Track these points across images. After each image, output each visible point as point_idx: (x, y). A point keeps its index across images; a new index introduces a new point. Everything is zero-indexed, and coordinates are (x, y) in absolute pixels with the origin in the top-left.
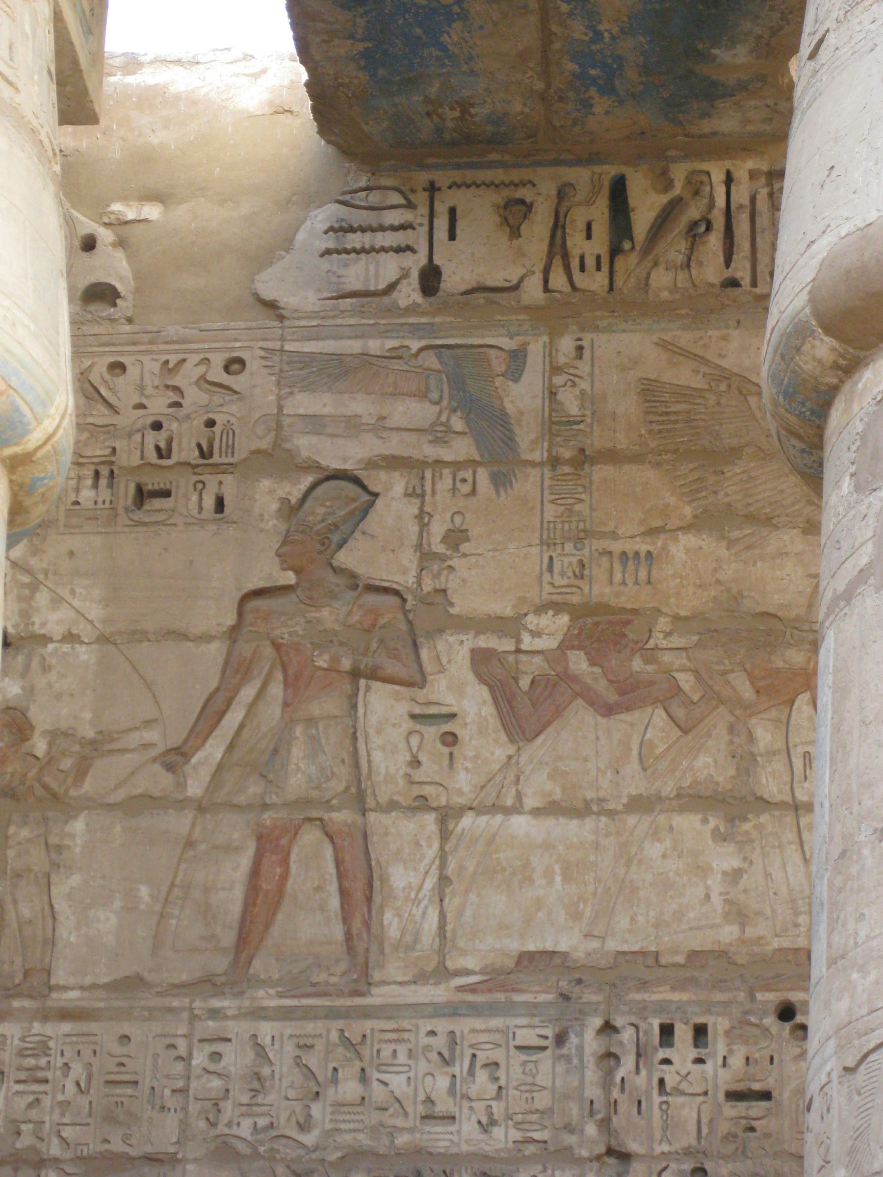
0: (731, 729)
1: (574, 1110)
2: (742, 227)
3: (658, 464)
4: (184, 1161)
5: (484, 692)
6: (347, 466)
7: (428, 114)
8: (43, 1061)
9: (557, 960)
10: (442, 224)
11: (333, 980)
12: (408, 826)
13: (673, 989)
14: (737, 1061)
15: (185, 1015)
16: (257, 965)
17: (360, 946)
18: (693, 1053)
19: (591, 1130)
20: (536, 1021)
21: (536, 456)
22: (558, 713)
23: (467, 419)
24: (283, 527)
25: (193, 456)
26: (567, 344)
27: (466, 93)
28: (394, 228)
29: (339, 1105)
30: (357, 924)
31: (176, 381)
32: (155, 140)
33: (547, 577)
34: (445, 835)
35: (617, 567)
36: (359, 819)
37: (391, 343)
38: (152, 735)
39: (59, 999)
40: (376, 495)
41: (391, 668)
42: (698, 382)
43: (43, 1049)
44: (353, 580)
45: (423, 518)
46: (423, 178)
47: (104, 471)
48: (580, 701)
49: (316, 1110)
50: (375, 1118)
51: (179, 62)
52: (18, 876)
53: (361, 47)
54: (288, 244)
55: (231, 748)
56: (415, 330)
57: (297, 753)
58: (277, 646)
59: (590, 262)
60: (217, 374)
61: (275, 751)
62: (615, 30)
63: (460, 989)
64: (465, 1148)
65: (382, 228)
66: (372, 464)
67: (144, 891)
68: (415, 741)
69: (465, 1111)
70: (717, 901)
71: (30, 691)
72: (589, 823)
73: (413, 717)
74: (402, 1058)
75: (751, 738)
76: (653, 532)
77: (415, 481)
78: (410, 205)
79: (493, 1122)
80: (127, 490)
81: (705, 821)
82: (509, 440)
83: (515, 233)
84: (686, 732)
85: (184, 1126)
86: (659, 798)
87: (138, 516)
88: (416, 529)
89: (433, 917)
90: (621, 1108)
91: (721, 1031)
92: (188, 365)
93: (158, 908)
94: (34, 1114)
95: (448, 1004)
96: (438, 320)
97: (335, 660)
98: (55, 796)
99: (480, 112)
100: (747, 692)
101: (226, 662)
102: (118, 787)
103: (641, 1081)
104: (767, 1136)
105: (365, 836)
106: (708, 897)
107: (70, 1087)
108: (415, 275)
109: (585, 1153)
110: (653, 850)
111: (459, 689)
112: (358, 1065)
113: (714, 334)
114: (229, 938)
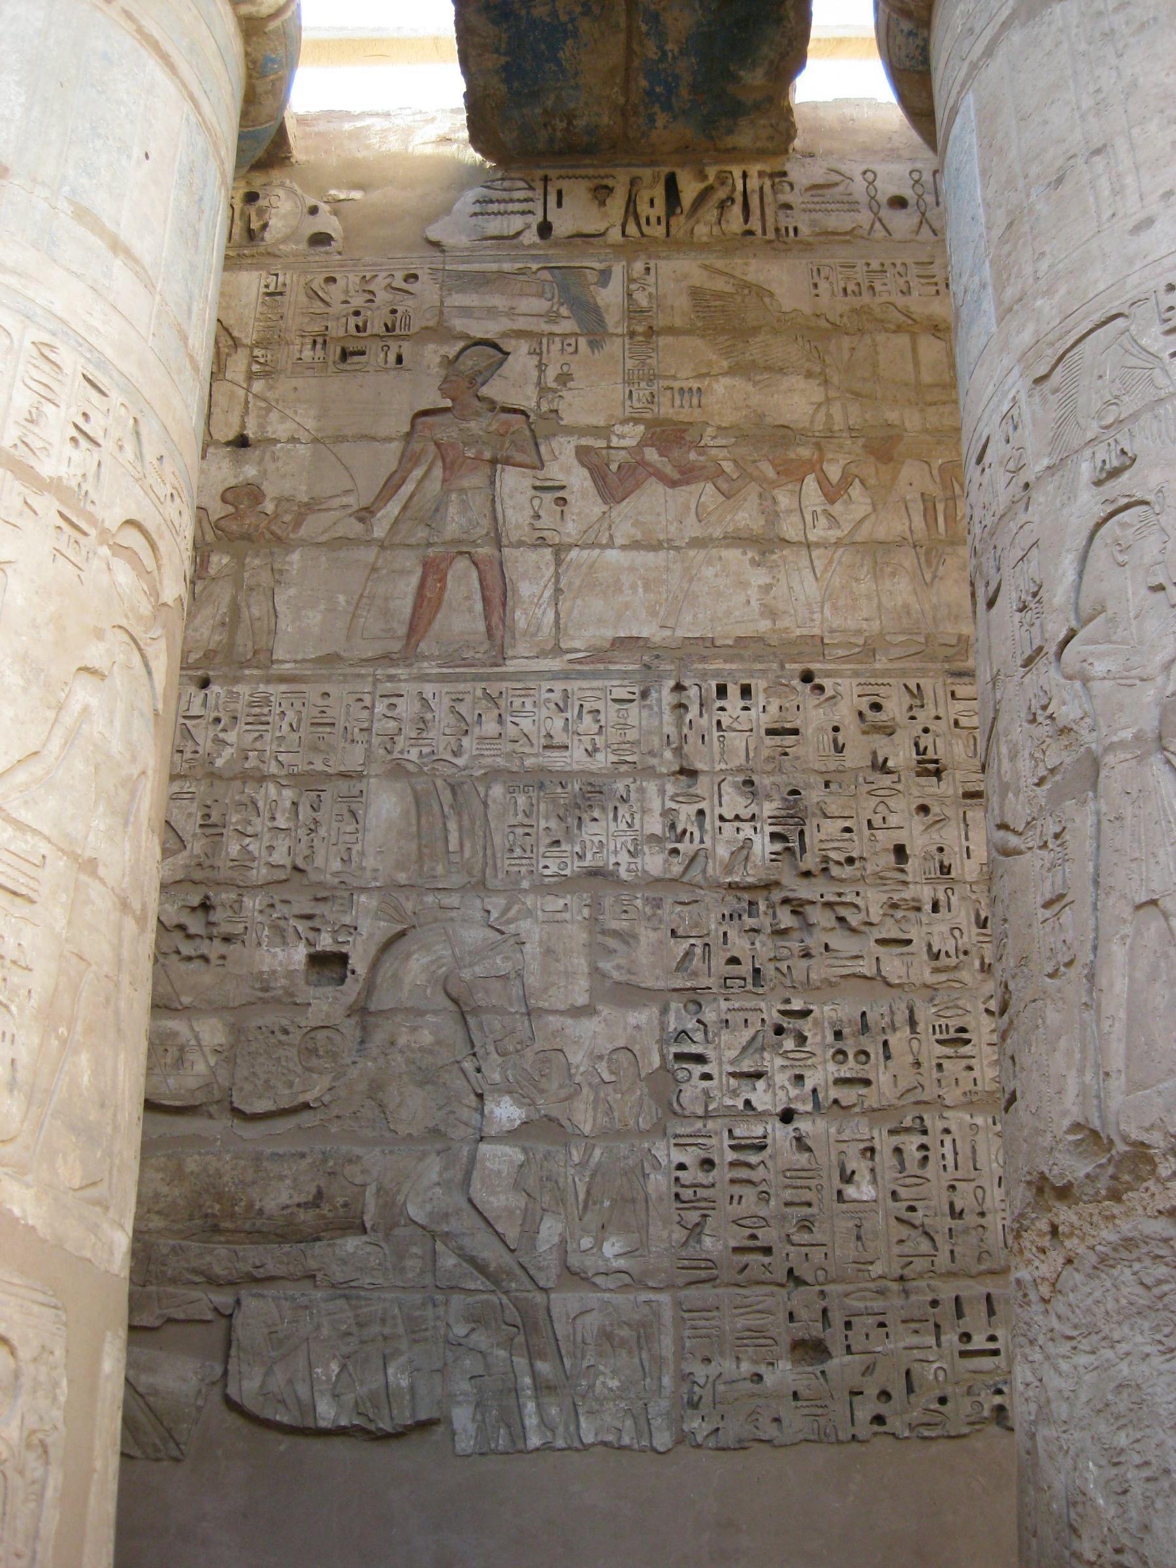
0: (760, 496)
1: (656, 742)
2: (754, 202)
3: (703, 337)
4: (368, 776)
5: (586, 472)
6: (488, 336)
7: (545, 125)
8: (266, 710)
9: (641, 643)
10: (552, 199)
11: (478, 656)
12: (532, 556)
13: (725, 661)
14: (773, 709)
15: (370, 679)
16: (423, 646)
17: (498, 634)
18: (742, 704)
19: (668, 754)
20: (626, 682)
21: (619, 331)
22: (638, 485)
23: (571, 309)
24: (443, 372)
25: (382, 331)
26: (639, 266)
27: (572, 105)
28: (519, 201)
29: (482, 739)
30: (495, 619)
31: (371, 288)
32: (359, 155)
33: (628, 403)
34: (558, 562)
35: (677, 397)
36: (496, 553)
37: (521, 265)
38: (350, 500)
39: (276, 669)
40: (508, 354)
41: (519, 457)
42: (728, 289)
43: (266, 701)
44: (492, 405)
45: (541, 367)
46: (540, 173)
47: (320, 340)
48: (653, 479)
49: (466, 742)
50: (510, 747)
51: (377, 115)
52: (251, 589)
53: (503, 60)
54: (447, 210)
55: (405, 508)
56: (535, 258)
57: (452, 510)
58: (438, 445)
59: (653, 220)
60: (399, 282)
61: (437, 510)
62: (676, 51)
63: (570, 661)
64: (575, 767)
65: (512, 201)
66: (505, 335)
67: (342, 599)
68: (536, 502)
69: (576, 743)
70: (754, 604)
71: (264, 473)
72: (662, 554)
73: (535, 488)
74: (528, 707)
75: (775, 501)
76: (700, 376)
77: (535, 345)
78: (531, 188)
79: (596, 750)
80: (335, 351)
81: (745, 553)
82: (601, 322)
83: (602, 203)
84: (728, 497)
85: (368, 753)
86: (711, 539)
87: (342, 366)
88: (535, 374)
89: (550, 616)
90: (690, 740)
91: (761, 689)
92: (379, 279)
93: (351, 609)
94: (258, 745)
95: (562, 671)
96: (550, 252)
97: (480, 452)
98: (279, 539)
99: (580, 123)
100: (771, 473)
101: (403, 455)
102: (323, 533)
103: (704, 721)
104: (798, 758)
105: (501, 564)
106: (748, 602)
107: (286, 727)
108: (534, 227)
109: (664, 770)
110: (709, 572)
111: (568, 470)
112: (496, 712)
113: (739, 261)
114: (402, 630)
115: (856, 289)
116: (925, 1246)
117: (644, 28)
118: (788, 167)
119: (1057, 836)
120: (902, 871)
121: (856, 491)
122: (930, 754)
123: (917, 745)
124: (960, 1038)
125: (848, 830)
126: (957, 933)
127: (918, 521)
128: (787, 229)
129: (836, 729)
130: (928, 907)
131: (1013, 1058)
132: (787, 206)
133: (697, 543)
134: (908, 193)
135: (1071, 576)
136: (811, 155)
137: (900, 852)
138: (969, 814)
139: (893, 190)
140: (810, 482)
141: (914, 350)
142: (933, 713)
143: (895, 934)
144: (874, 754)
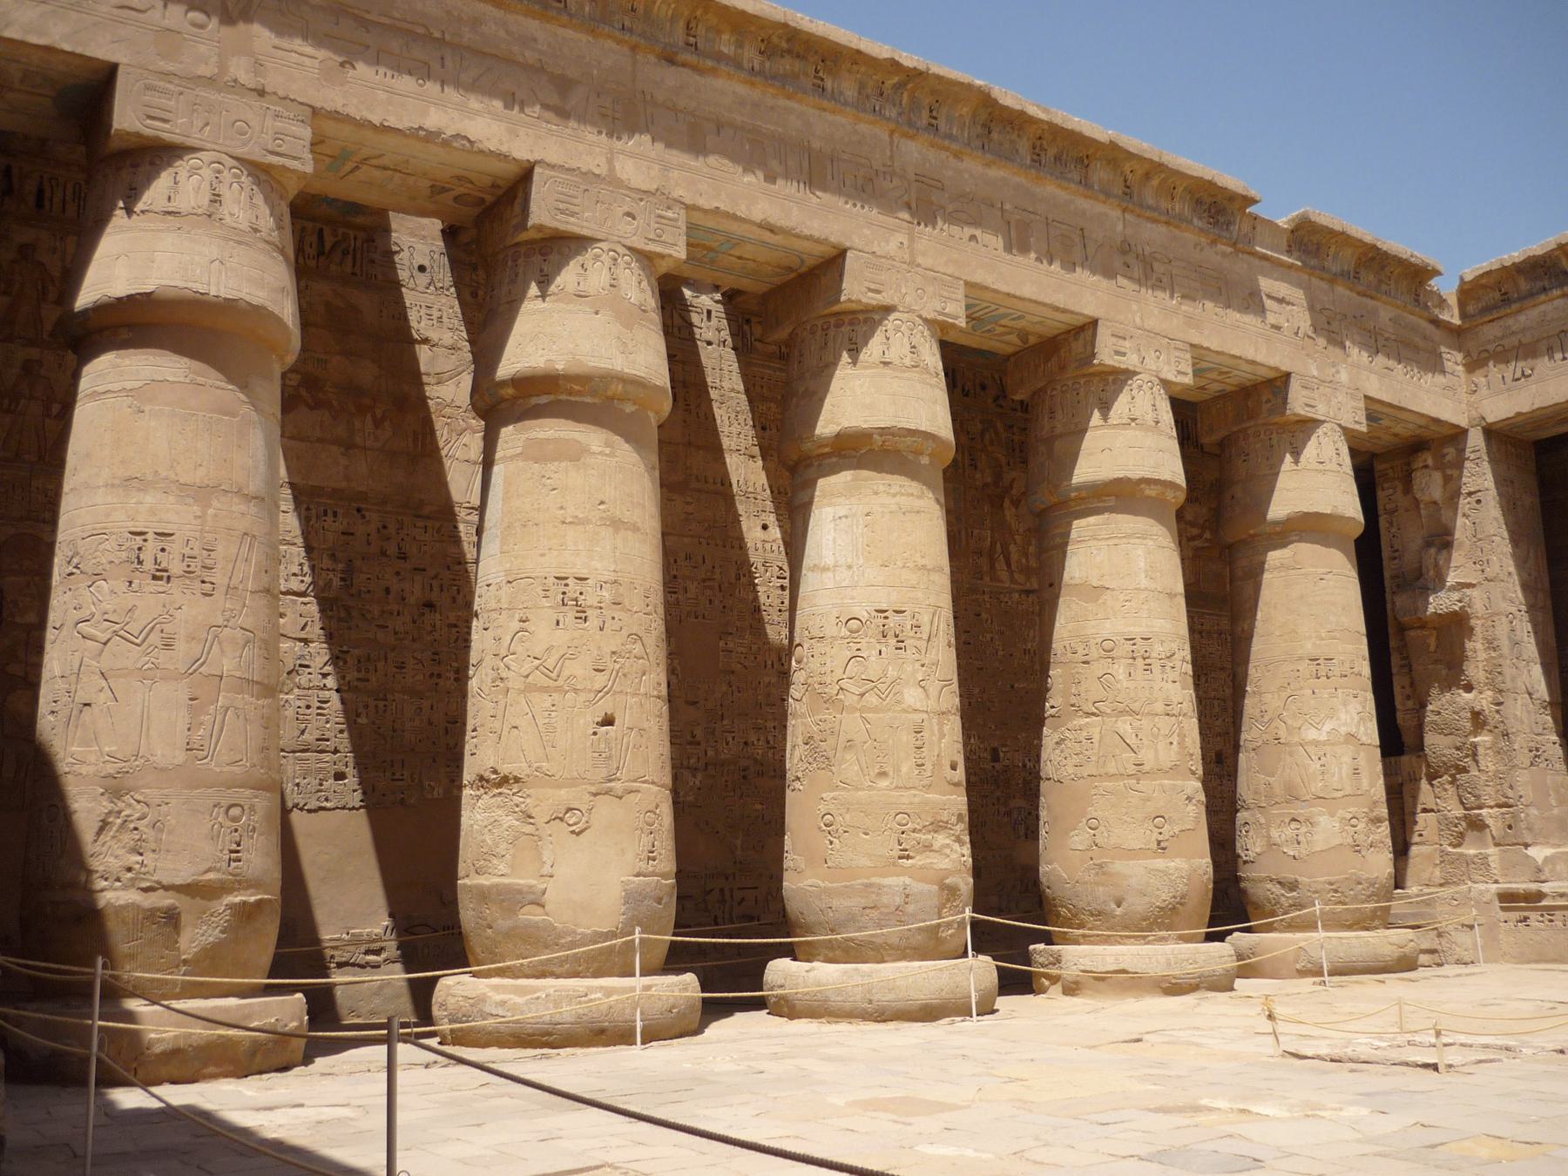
2: (358, 255)
116: (383, 742)
121: (387, 424)
124: (401, 667)
125: (369, 579)
129: (369, 535)
130: (395, 613)
132: (373, 262)
133: (320, 440)
134: (426, 263)
137: (387, 591)
140: (369, 417)
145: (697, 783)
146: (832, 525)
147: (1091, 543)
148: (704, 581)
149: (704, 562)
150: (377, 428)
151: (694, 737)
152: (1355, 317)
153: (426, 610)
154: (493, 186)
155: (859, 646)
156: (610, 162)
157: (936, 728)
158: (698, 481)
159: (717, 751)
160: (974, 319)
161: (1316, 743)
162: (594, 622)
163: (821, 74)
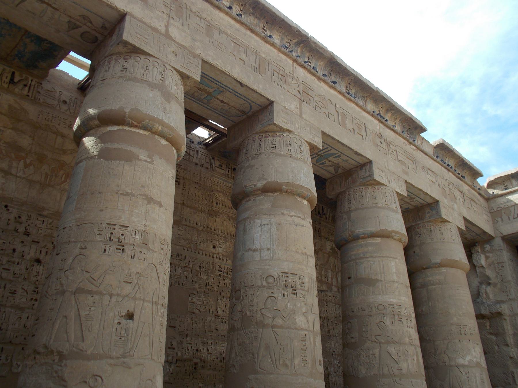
2: (32, 88)
59: (6, 82)
115: (48, 119)
117: (22, 45)
118: (43, 83)
119: (55, 300)
120: (13, 254)
121: (32, 167)
122: (28, 231)
123: (26, 228)
124: (14, 292)
125: (4, 243)
126: (21, 270)
127: (43, 179)
128: (37, 98)
129: (9, 220)
130: (16, 263)
131: (36, 329)
132: (39, 93)
134: (68, 101)
135: (71, 261)
136: (49, 82)
137: (14, 250)
138: (32, 246)
139: (65, 99)
140: (22, 162)
141: (56, 139)
142: (32, 222)
143: (7, 267)
144: (16, 228)
145: (171, 370)
146: (260, 228)
147: (370, 259)
148: (185, 267)
149: (185, 258)
150: (26, 168)
151: (172, 345)
152: (457, 186)
153: (37, 264)
154: (102, 27)
155: (272, 291)
156: (167, 27)
157: (312, 342)
158: (186, 221)
159: (182, 353)
160: (318, 155)
161: (463, 366)
162: (129, 252)
163: (265, 28)
